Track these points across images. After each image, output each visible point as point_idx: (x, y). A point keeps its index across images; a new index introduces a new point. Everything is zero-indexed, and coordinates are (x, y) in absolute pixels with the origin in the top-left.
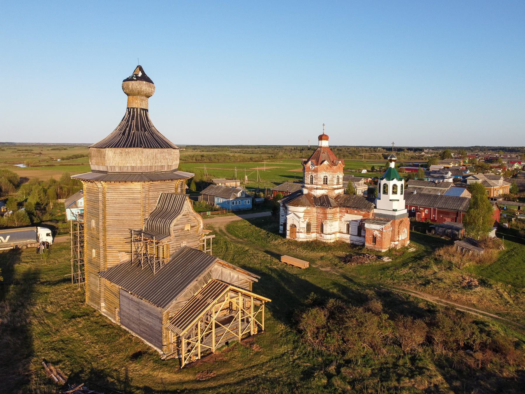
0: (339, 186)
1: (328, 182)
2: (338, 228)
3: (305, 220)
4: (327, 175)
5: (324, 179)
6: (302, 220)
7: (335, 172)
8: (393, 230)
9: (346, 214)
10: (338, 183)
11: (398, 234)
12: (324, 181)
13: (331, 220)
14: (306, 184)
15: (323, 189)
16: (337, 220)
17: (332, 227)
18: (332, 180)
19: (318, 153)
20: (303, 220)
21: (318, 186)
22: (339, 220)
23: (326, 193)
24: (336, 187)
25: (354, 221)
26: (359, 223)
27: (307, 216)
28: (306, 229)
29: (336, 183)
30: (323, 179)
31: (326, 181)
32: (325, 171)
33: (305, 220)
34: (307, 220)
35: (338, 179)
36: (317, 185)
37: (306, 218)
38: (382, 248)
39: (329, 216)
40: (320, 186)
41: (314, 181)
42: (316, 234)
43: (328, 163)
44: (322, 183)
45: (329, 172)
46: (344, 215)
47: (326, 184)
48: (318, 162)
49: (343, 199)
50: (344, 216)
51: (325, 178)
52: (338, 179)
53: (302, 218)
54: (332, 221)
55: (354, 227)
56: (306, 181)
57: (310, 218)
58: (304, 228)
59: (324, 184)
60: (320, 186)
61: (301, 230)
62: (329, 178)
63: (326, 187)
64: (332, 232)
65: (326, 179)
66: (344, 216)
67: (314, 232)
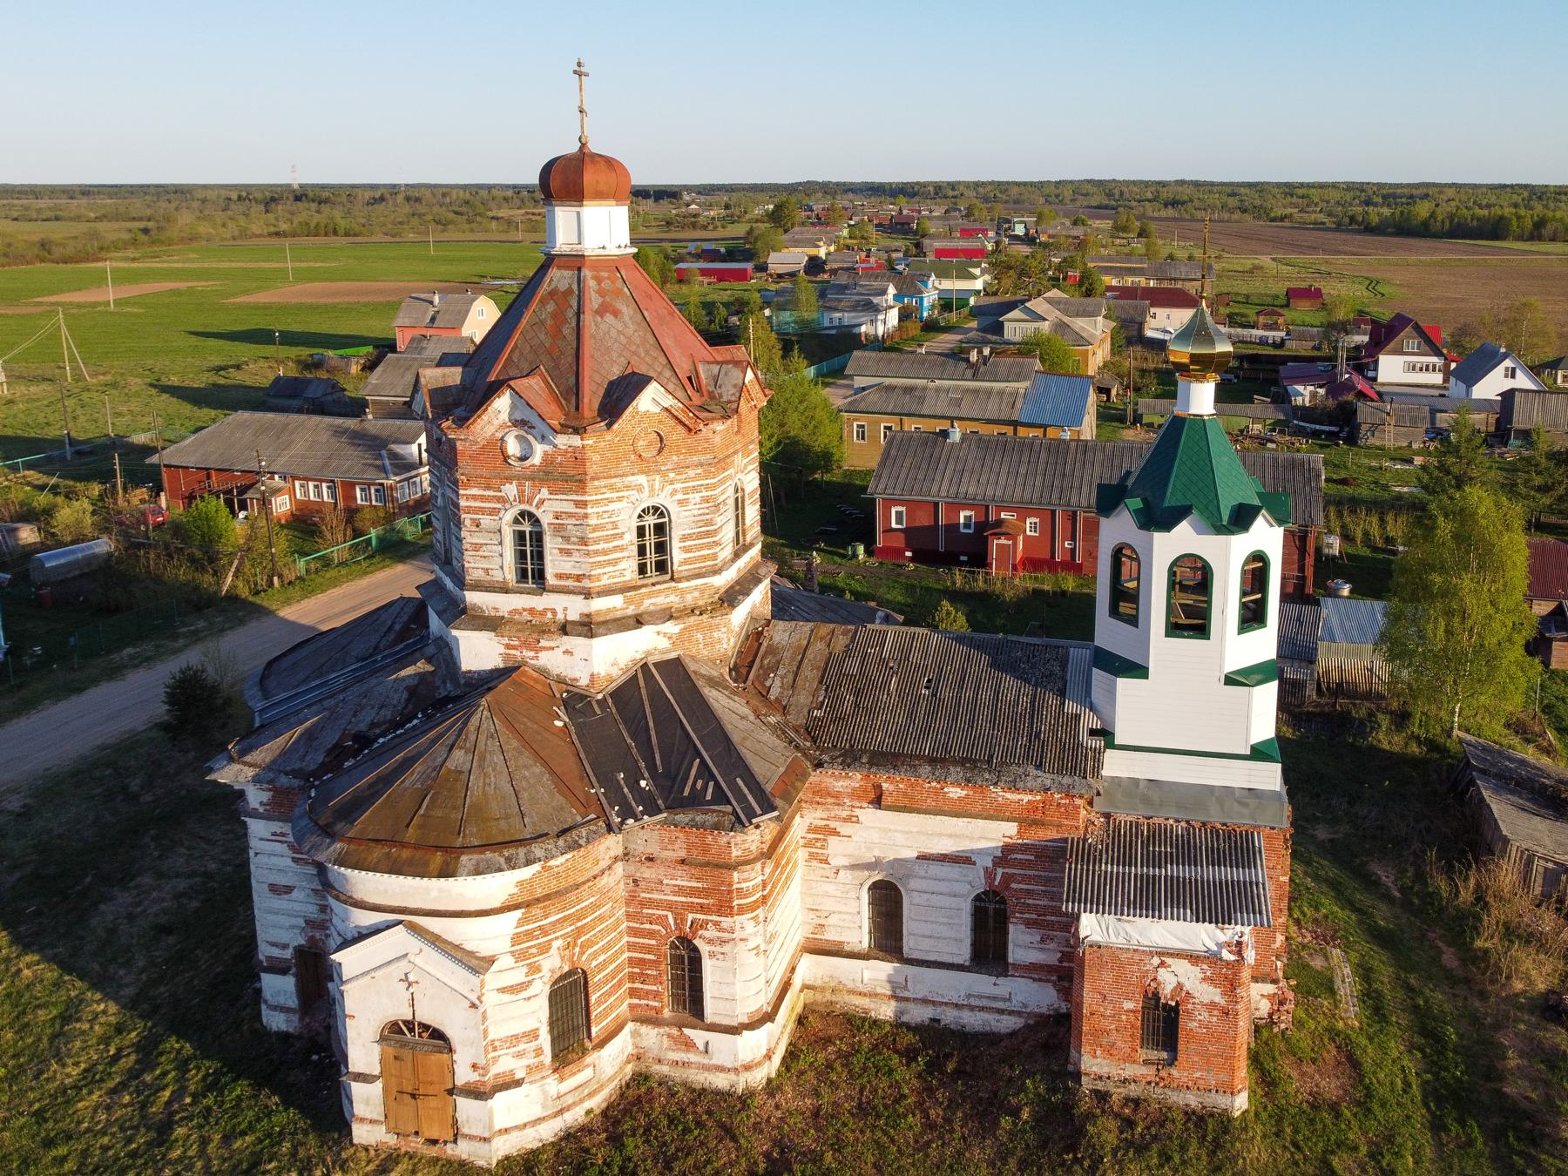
1: (677, 555)
5: (641, 532)
9: (869, 815)
12: (642, 551)
14: (478, 587)
15: (638, 621)
19: (559, 317)
21: (599, 605)
23: (664, 644)
25: (943, 858)
26: (989, 874)
30: (631, 537)
31: (661, 548)
36: (588, 595)
40: (615, 602)
41: (554, 564)
44: (628, 568)
45: (679, 468)
47: (661, 567)
48: (572, 393)
49: (810, 674)
51: (651, 520)
55: (953, 902)
56: (474, 566)
59: (642, 569)
60: (615, 602)
63: (662, 596)
65: (660, 529)
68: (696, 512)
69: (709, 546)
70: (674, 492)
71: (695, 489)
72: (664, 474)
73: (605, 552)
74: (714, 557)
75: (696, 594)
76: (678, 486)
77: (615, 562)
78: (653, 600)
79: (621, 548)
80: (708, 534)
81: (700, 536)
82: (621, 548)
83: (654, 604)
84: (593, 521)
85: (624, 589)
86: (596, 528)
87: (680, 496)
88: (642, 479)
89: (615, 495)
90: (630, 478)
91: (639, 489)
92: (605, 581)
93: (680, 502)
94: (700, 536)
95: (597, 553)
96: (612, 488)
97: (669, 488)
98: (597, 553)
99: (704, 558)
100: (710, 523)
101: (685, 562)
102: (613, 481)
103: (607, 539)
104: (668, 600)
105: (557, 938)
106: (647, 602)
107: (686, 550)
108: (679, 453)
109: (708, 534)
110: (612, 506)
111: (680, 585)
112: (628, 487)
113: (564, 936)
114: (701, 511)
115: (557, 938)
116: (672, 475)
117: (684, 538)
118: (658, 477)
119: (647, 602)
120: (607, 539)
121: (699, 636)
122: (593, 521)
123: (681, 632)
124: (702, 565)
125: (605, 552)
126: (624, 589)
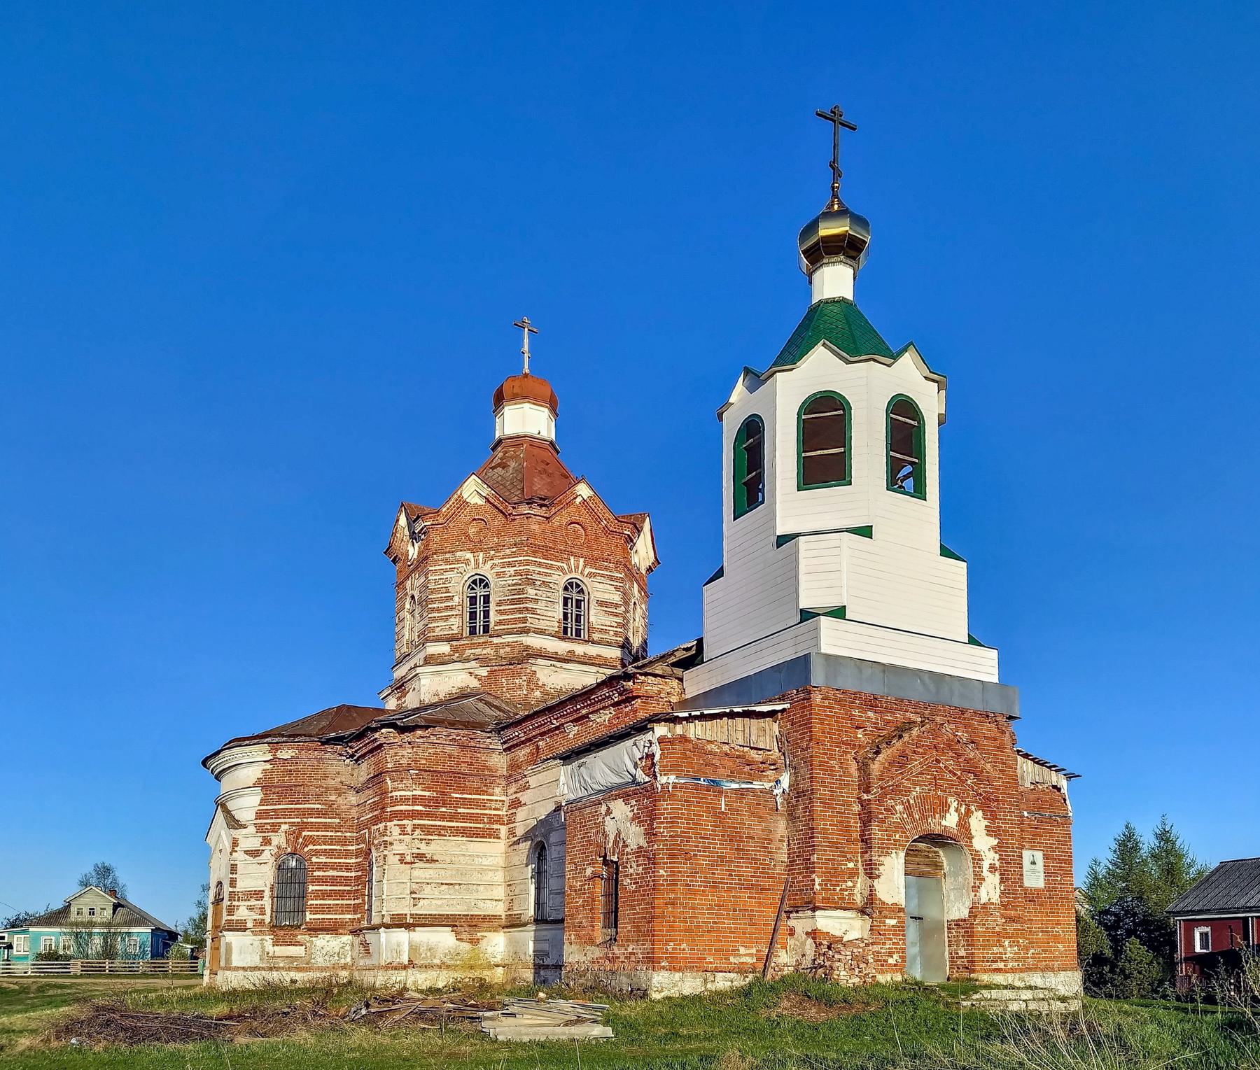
0: (580, 649)
1: (493, 617)
2: (500, 892)
3: (267, 842)
4: (486, 571)
5: (473, 600)
6: (249, 838)
7: (547, 550)
8: (798, 794)
10: (573, 627)
11: (866, 841)
12: (473, 615)
13: (412, 815)
16: (491, 834)
17: (422, 872)
18: (518, 600)
20: (255, 843)
22: (503, 830)
23: (474, 683)
24: (562, 647)
27: (278, 814)
28: (267, 902)
29: (555, 627)
32: (475, 546)
33: (267, 842)
34: (278, 839)
35: (574, 595)
37: (275, 828)
38: (651, 961)
39: (405, 790)
40: (444, 648)
42: (348, 938)
43: (486, 491)
44: (456, 624)
45: (499, 548)
46: (525, 788)
47: (486, 629)
50: (525, 797)
52: (574, 595)
53: (252, 829)
54: (428, 830)
57: (303, 826)
58: (259, 894)
59: (473, 631)
60: (444, 648)
61: (242, 913)
62: (498, 589)
64: (424, 908)
65: (487, 599)
66: (525, 797)
67: (333, 929)
68: (510, 582)
69: (520, 611)
70: (492, 568)
71: (510, 564)
72: (486, 551)
73: (439, 610)
74: (525, 620)
75: (508, 649)
76: (496, 562)
77: (446, 618)
78: (473, 651)
79: (452, 608)
80: (520, 601)
81: (512, 602)
82: (452, 608)
83: (474, 654)
84: (432, 586)
85: (449, 639)
86: (434, 591)
87: (498, 569)
88: (469, 555)
89: (448, 567)
90: (459, 554)
91: (467, 562)
92: (438, 632)
93: (498, 574)
94: (512, 602)
95: (433, 610)
96: (447, 562)
97: (490, 564)
98: (433, 610)
99: (515, 621)
100: (521, 592)
101: (499, 623)
102: (448, 555)
103: (441, 600)
104: (485, 652)
105: (285, 823)
106: (468, 652)
107: (501, 613)
108: (499, 536)
109: (520, 601)
110: (447, 575)
111: (495, 640)
112: (458, 561)
113: (292, 824)
114: (514, 582)
115: (285, 823)
116: (492, 552)
117: (499, 604)
118: (481, 554)
119: (468, 652)
120: (441, 600)
121: (503, 680)
122: (432, 586)
123: (491, 672)
124: (513, 626)
125: (439, 610)
126: (449, 639)
